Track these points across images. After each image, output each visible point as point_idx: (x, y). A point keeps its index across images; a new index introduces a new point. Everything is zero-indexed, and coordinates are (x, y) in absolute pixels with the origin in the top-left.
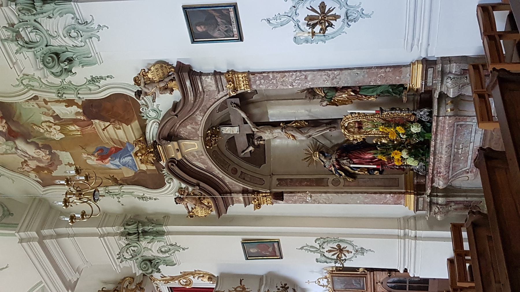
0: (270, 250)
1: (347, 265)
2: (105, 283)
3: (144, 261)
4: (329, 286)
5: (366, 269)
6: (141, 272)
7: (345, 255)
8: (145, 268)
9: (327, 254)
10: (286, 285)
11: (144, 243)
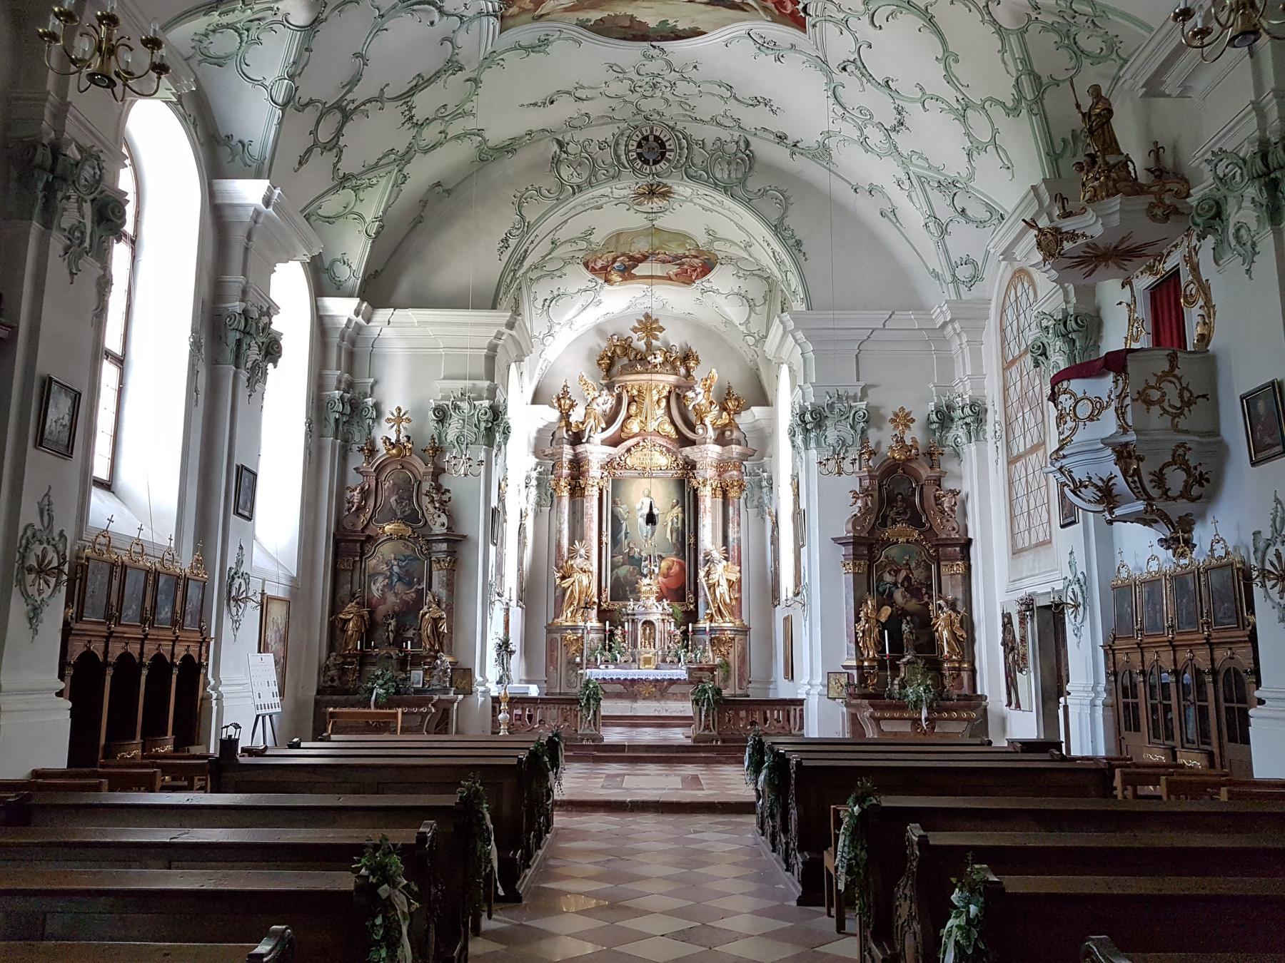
0: (1268, 440)
1: (1257, 591)
2: (1175, 148)
3: (1217, 203)
4: (1214, 561)
5: (1254, 628)
6: (1195, 204)
7: (1274, 586)
8: (1202, 209)
9: (1271, 551)
10: (1208, 480)
11: (1251, 192)
